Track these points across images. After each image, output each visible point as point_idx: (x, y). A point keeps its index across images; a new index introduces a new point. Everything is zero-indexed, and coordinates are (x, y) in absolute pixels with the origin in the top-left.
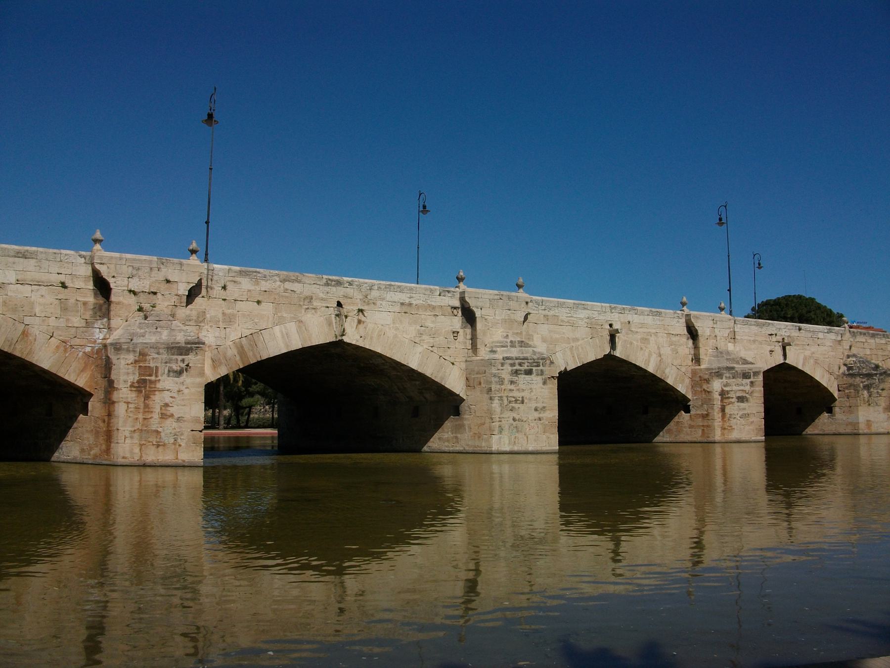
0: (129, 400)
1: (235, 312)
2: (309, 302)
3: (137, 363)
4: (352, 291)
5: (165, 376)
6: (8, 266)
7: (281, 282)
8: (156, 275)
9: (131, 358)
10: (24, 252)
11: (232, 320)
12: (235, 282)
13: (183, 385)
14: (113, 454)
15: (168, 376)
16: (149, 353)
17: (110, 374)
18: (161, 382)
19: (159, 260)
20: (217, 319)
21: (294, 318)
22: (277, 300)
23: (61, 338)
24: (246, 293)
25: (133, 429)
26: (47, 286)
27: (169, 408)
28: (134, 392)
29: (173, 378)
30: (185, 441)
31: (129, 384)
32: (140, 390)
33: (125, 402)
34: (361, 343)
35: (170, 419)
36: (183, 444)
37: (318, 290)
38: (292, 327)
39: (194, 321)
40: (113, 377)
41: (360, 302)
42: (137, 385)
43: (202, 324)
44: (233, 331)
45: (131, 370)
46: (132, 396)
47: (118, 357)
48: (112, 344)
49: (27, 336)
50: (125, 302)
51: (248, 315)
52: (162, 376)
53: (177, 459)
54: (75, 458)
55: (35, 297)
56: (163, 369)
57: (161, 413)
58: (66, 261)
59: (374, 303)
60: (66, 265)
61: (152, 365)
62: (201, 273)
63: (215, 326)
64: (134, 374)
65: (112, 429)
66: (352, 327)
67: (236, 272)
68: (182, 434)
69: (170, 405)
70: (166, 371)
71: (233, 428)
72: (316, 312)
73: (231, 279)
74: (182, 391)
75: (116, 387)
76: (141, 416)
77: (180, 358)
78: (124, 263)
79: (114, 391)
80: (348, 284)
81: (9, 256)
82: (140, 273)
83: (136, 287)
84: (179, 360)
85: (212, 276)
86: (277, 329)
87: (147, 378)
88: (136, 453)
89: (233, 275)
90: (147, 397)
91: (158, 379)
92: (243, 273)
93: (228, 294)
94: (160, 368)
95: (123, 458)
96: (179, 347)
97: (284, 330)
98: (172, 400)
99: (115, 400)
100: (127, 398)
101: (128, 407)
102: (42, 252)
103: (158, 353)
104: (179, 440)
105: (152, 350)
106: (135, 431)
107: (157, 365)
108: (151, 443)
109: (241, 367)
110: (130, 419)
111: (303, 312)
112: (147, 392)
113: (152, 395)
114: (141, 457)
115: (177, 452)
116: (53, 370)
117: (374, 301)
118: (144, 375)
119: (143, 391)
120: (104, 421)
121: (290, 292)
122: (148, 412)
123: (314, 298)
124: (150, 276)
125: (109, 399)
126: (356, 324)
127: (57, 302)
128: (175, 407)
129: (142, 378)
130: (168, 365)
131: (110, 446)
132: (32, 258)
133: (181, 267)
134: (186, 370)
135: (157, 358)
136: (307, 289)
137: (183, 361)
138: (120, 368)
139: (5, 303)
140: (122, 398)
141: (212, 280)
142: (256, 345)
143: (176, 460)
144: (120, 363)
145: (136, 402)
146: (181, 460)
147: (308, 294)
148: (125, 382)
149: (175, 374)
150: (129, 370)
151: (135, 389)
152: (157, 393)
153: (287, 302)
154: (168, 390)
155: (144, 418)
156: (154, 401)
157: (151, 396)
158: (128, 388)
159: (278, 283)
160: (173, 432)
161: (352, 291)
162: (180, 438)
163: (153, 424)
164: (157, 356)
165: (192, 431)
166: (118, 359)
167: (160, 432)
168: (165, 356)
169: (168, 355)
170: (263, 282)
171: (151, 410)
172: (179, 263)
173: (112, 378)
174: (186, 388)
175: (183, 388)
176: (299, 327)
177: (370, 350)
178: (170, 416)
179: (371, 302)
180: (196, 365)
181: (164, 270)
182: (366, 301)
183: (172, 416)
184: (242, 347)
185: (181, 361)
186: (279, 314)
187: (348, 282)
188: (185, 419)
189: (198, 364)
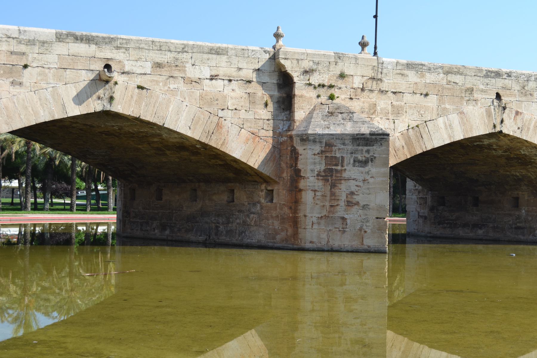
0: (316, 188)
1: (403, 104)
2: (470, 94)
3: (323, 154)
4: (510, 82)
5: (351, 166)
6: (203, 63)
7: (444, 74)
8: (334, 69)
9: (317, 148)
10: (217, 49)
11: (400, 112)
12: (402, 75)
13: (369, 174)
14: (301, 239)
15: (354, 166)
16: (335, 144)
17: (296, 164)
18: (347, 172)
19: (336, 55)
20: (387, 112)
21: (457, 110)
22: (441, 92)
23: (249, 129)
24: (412, 85)
25: (320, 216)
26: (237, 80)
27: (355, 197)
28: (321, 181)
29: (359, 168)
30: (370, 227)
31: (316, 173)
32: (326, 179)
33: (312, 190)
34: (518, 135)
35: (356, 207)
36: (369, 231)
37: (479, 81)
38: (454, 118)
39: (366, 113)
40: (300, 166)
41: (517, 93)
42: (324, 175)
43: (373, 116)
44: (401, 122)
45: (318, 160)
46: (319, 184)
47: (305, 147)
48: (298, 136)
49: (221, 128)
50: (308, 95)
51: (415, 107)
52: (347, 165)
53: (362, 244)
54: (259, 241)
55: (227, 91)
56: (349, 159)
57: (347, 201)
58: (253, 56)
59: (531, 95)
60: (253, 60)
61: (338, 155)
62: (374, 66)
63: (385, 117)
64: (320, 163)
65: (299, 215)
66: (510, 119)
67: (403, 65)
68: (368, 221)
69: (356, 193)
70: (352, 161)
71: (391, 217)
72: (476, 104)
73: (399, 72)
74: (367, 180)
75: (303, 176)
76: (327, 204)
77: (365, 148)
78: (306, 58)
79: (300, 180)
80: (506, 75)
81: (203, 53)
82: (320, 67)
83: (317, 81)
84: (364, 150)
85: (382, 69)
86: (441, 120)
87: (334, 167)
88: (323, 238)
89: (400, 68)
90: (333, 186)
91: (343, 168)
92: (410, 66)
93: (396, 87)
94: (346, 158)
95: (311, 242)
96: (364, 138)
97: (447, 122)
98: (357, 188)
99: (302, 188)
100: (314, 186)
101: (315, 194)
102: (232, 49)
103: (344, 144)
104: (364, 227)
105: (338, 141)
106: (322, 217)
107: (343, 156)
108: (338, 230)
109: (409, 157)
110: (318, 206)
111: (465, 104)
112: (333, 181)
113: (337, 183)
114: (328, 242)
115: (363, 238)
116: (244, 160)
117: (531, 93)
118: (330, 165)
119: (330, 180)
120: (291, 208)
121: (453, 84)
122: (334, 199)
123: (475, 89)
124: (328, 70)
125: (297, 187)
126: (514, 115)
127: (246, 96)
128: (361, 195)
129: (328, 167)
130: (354, 155)
131: (298, 230)
132: (224, 54)
133: (356, 61)
134: (372, 161)
135: (342, 148)
136: (468, 81)
137: (368, 151)
138: (307, 158)
139: (201, 97)
140: (309, 186)
141: (381, 73)
142: (422, 137)
143: (362, 246)
144: (307, 153)
145: (323, 190)
146: (366, 245)
147: (468, 86)
148: (312, 171)
149: (360, 164)
150: (315, 160)
151: (322, 178)
152: (343, 182)
153: (450, 94)
154: (353, 179)
155: (330, 206)
156: (341, 189)
157: (338, 185)
158: (315, 176)
159: (442, 75)
160: (359, 219)
161: (510, 82)
162: (366, 225)
163: (340, 212)
164: (342, 147)
165: (377, 218)
166: (304, 149)
167: (346, 219)
168: (350, 147)
169: (353, 146)
170: (428, 75)
171: (337, 198)
172: (354, 57)
173: (299, 168)
174: (371, 177)
175: (368, 177)
176: (462, 118)
177: (526, 141)
178: (355, 204)
179: (528, 93)
180: (381, 156)
181: (340, 64)
182: (524, 92)
183: (357, 203)
184: (409, 138)
185: (366, 151)
186: (443, 106)
187: (505, 73)
188: (370, 207)
189: (384, 154)
